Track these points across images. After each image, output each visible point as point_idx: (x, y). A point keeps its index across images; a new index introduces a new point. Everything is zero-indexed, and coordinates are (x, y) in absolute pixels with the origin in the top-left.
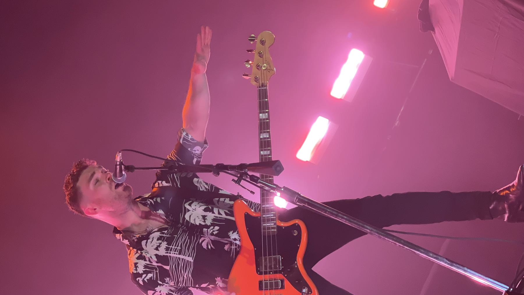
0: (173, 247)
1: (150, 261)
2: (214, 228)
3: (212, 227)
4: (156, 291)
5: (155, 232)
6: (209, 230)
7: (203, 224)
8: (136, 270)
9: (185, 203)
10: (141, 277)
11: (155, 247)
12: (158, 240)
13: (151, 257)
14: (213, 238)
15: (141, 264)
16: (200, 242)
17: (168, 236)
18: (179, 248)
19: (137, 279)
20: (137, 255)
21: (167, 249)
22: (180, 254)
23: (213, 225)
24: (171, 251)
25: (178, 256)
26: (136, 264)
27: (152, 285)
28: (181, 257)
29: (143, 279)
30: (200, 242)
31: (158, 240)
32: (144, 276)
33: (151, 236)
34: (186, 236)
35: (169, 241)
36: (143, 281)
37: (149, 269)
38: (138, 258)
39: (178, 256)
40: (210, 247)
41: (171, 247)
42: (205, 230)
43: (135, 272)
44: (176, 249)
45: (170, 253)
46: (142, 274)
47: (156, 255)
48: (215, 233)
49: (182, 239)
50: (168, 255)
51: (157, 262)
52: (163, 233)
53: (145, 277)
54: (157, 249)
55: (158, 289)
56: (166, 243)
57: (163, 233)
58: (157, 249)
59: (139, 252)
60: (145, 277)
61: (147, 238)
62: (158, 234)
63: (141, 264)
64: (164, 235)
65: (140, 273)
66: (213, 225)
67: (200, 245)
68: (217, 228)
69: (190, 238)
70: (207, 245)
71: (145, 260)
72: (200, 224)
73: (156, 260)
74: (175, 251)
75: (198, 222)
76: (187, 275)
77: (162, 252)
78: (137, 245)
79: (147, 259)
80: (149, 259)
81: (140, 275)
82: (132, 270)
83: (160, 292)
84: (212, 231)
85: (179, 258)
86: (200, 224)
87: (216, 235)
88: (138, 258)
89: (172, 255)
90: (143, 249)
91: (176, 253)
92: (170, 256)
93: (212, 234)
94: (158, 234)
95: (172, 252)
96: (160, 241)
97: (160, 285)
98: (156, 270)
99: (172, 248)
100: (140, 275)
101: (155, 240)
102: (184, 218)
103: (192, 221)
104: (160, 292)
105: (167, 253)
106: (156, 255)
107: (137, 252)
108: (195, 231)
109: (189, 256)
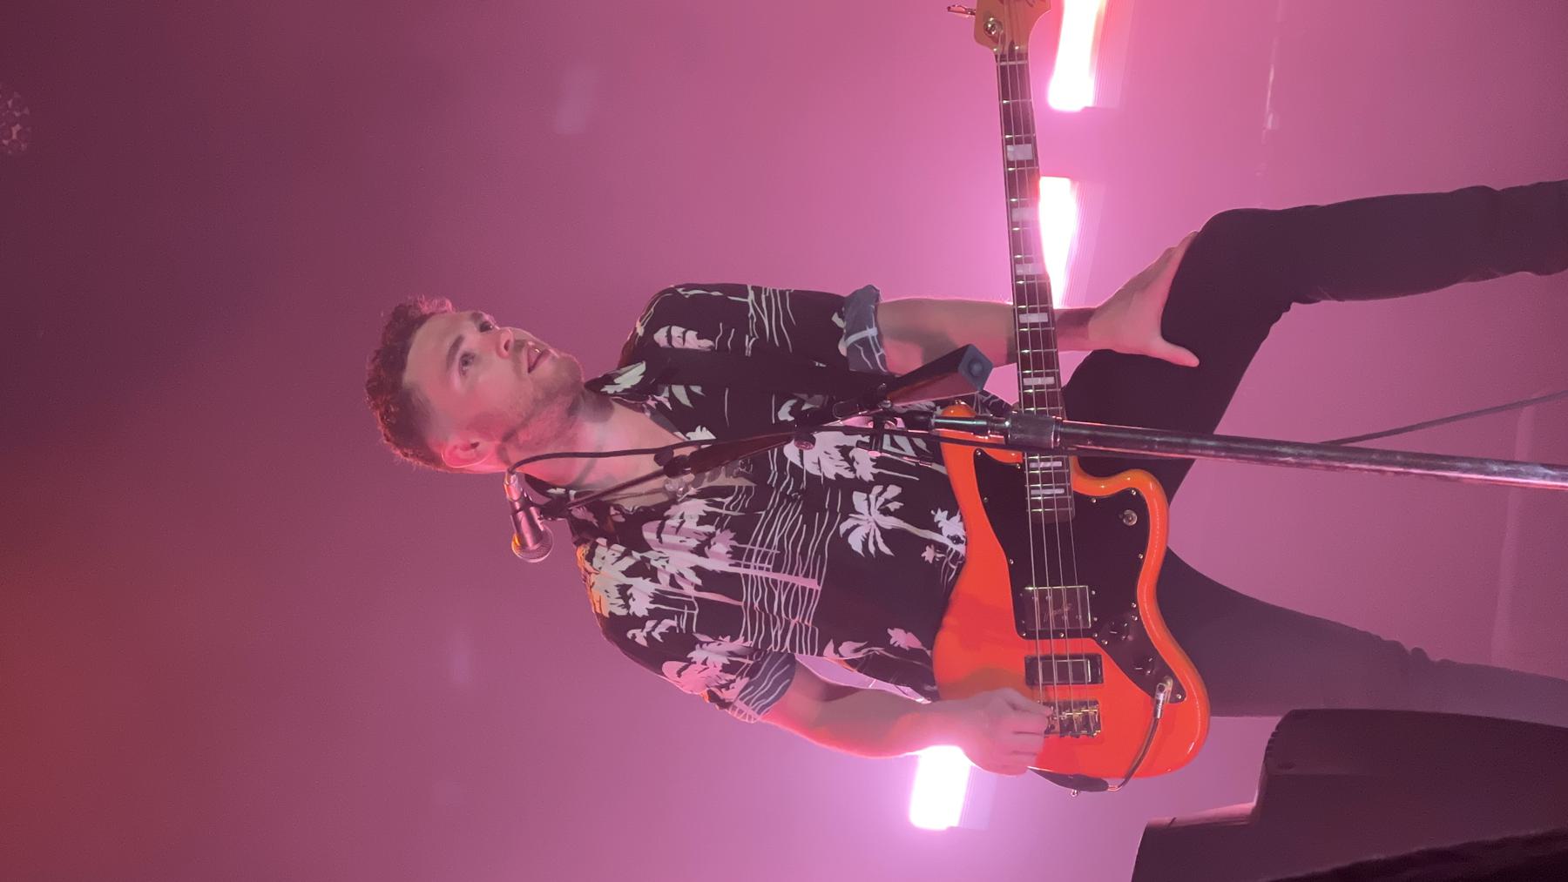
0: (756, 548)
1: (673, 582)
2: (884, 490)
3: (877, 489)
4: (690, 662)
6: (872, 497)
7: (848, 475)
8: (627, 606)
9: (778, 409)
11: (693, 543)
12: (699, 524)
13: (682, 575)
14: (891, 523)
15: (643, 591)
17: (736, 513)
19: (629, 635)
20: (627, 562)
21: (736, 554)
22: (777, 569)
23: (880, 480)
24: (749, 558)
25: (772, 575)
26: (624, 591)
27: (679, 647)
28: (781, 577)
29: (649, 633)
30: (844, 528)
31: (699, 524)
32: (650, 624)
33: (674, 511)
34: (795, 515)
35: (742, 529)
36: (649, 637)
38: (629, 573)
39: (772, 575)
40: (872, 549)
41: (749, 546)
42: (858, 498)
43: (622, 612)
44: (765, 554)
45: (747, 567)
46: (644, 619)
47: (698, 570)
48: (894, 506)
50: (741, 571)
51: (697, 588)
52: (720, 505)
54: (699, 551)
55: (697, 655)
57: (720, 505)
58: (699, 551)
59: (637, 556)
61: (657, 513)
62: (698, 507)
63: (643, 591)
64: (724, 511)
65: (639, 614)
66: (880, 480)
67: (841, 542)
68: (894, 490)
69: (808, 521)
70: (865, 544)
71: (655, 580)
72: (837, 475)
73: (699, 582)
74: (763, 561)
75: (832, 468)
77: (718, 561)
78: (629, 534)
79: (664, 579)
80: (672, 576)
81: (639, 622)
83: (704, 663)
84: (882, 500)
85: (775, 582)
86: (837, 475)
87: (896, 514)
88: (629, 573)
90: (646, 547)
91: (766, 565)
92: (746, 576)
93: (885, 511)
94: (698, 507)
95: (752, 564)
96: (709, 529)
97: (701, 643)
99: (751, 551)
100: (639, 622)
101: (691, 524)
102: (782, 459)
103: (810, 467)
104: (704, 663)
105: (738, 565)
106: (698, 570)
109: (806, 576)
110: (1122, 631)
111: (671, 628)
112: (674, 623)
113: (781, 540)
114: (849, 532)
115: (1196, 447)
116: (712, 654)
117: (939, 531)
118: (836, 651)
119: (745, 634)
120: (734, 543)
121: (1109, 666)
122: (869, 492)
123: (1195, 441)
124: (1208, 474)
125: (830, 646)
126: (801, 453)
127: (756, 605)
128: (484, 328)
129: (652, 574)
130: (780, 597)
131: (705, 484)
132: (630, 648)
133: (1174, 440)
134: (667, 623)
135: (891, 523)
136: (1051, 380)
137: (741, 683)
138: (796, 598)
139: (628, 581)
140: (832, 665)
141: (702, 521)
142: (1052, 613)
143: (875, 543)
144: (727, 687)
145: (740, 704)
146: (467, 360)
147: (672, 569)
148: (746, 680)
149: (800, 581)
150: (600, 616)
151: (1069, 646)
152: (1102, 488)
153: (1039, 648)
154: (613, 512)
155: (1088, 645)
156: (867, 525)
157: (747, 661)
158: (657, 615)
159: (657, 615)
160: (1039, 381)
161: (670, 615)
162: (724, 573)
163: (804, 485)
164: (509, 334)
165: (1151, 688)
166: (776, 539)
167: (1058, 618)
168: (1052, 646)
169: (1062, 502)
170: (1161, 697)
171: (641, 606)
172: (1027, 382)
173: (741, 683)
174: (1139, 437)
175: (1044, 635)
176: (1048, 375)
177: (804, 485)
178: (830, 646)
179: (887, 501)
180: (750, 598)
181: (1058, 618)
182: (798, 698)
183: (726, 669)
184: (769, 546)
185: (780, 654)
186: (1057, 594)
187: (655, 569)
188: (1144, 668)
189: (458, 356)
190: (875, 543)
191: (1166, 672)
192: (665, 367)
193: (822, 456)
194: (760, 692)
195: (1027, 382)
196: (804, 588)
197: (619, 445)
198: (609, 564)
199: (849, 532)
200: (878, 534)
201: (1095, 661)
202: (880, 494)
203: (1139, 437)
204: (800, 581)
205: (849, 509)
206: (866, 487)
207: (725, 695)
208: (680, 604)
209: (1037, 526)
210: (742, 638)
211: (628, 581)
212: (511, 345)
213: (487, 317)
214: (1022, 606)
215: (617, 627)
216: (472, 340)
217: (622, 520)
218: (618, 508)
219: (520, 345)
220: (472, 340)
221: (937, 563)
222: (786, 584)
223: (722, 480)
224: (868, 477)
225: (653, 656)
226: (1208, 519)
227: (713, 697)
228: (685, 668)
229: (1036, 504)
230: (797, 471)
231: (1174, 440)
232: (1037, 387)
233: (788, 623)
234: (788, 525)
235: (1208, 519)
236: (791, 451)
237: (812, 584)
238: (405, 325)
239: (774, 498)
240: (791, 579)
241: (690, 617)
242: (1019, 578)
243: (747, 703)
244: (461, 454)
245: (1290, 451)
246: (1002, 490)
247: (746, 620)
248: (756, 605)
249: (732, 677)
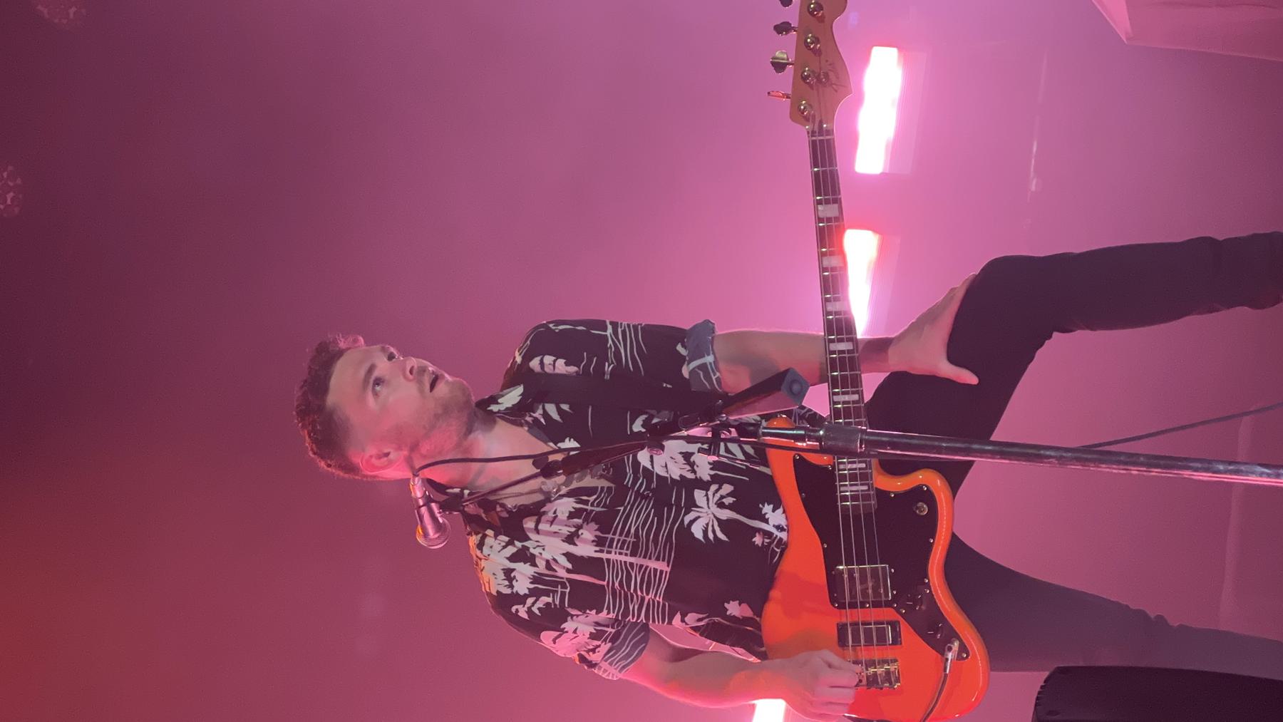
0: (617, 537)
1: (548, 566)
3: (714, 487)
4: (563, 631)
5: (562, 496)
6: (710, 493)
7: (690, 476)
8: (511, 586)
9: (633, 422)
10: (524, 603)
13: (555, 560)
14: (726, 514)
16: (686, 522)
18: (631, 539)
20: (511, 550)
21: (599, 542)
22: (633, 554)
24: (610, 546)
25: (630, 559)
26: (508, 573)
27: (554, 619)
29: (529, 608)
30: (687, 519)
32: (530, 601)
33: (550, 508)
35: (604, 522)
36: (529, 611)
37: (543, 583)
39: (630, 559)
40: (711, 536)
41: (610, 536)
43: (508, 591)
44: (624, 542)
45: (609, 552)
46: (526, 596)
47: (568, 555)
49: (637, 518)
50: (604, 556)
51: (568, 571)
52: (586, 502)
53: (533, 604)
54: (570, 539)
55: (569, 625)
56: (594, 526)
57: (586, 502)
58: (570, 539)
59: (519, 544)
60: (533, 604)
61: (536, 510)
62: (565, 506)
63: (524, 571)
64: (589, 508)
65: (522, 593)
66: (715, 479)
67: (686, 531)
68: (727, 488)
69: (659, 515)
70: (705, 532)
71: (534, 565)
72: (681, 476)
73: (570, 566)
74: (622, 548)
75: (677, 471)
76: (656, 596)
77: (585, 549)
78: (512, 525)
79: (541, 564)
80: (548, 561)
81: (521, 599)
82: (497, 585)
83: (575, 632)
84: (718, 495)
85: (632, 564)
86: (681, 476)
87: (730, 507)
88: (513, 558)
89: (612, 557)
90: (528, 539)
92: (608, 560)
93: (721, 505)
96: (579, 521)
97: (572, 616)
98: (564, 586)
99: (612, 540)
100: (521, 599)
102: (636, 464)
103: (659, 470)
104: (575, 632)
105: (602, 551)
106: (568, 555)
107: (508, 544)
108: (673, 496)
109: (658, 559)
110: (916, 602)
111: (548, 604)
112: (550, 600)
113: (637, 530)
114: (692, 522)
116: (580, 626)
117: (766, 521)
118: (683, 621)
119: (608, 608)
120: (598, 533)
121: (906, 630)
122: (707, 490)
123: (976, 446)
124: (984, 469)
125: (678, 616)
126: (652, 457)
127: (617, 584)
129: (531, 560)
130: (636, 577)
131: (575, 485)
132: (515, 620)
133: (958, 445)
134: (545, 599)
135: (726, 514)
136: (856, 397)
137: (605, 647)
138: (649, 580)
139: (512, 565)
140: (681, 630)
141: (572, 515)
142: (858, 587)
143: (714, 531)
144: (593, 651)
145: (605, 665)
147: (547, 555)
148: (609, 645)
149: (653, 564)
150: (489, 594)
151: (873, 614)
152: (898, 485)
153: (848, 616)
154: (499, 509)
155: (888, 614)
156: (707, 517)
157: (610, 630)
158: (535, 593)
159: (535, 593)
160: (846, 398)
161: (547, 593)
162: (590, 558)
163: (654, 485)
164: (413, 362)
165: (941, 648)
166: (633, 530)
167: (864, 592)
168: (859, 615)
169: (866, 497)
170: (950, 656)
171: (522, 586)
172: (836, 398)
173: (605, 647)
174: (928, 443)
175: (853, 606)
176: (853, 393)
177: (654, 485)
178: (678, 616)
179: (722, 497)
180: (611, 580)
181: (864, 592)
182: (651, 659)
183: (593, 636)
184: (627, 536)
185: (636, 624)
186: (863, 572)
187: (533, 556)
188: (936, 632)
190: (714, 531)
191: (952, 635)
192: (540, 390)
193: (667, 460)
194: (621, 654)
195: (836, 398)
196: (655, 570)
197: (505, 454)
198: (495, 554)
199: (692, 522)
200: (716, 524)
201: (894, 625)
202: (717, 491)
203: (928, 443)
204: (653, 564)
205: (691, 504)
206: (704, 486)
207: (593, 657)
208: (555, 584)
209: (846, 517)
210: (605, 611)
211: (512, 565)
214: (834, 581)
215: (504, 602)
216: (383, 367)
217: (505, 515)
218: (503, 506)
219: (423, 370)
220: (383, 367)
221: (765, 548)
222: (641, 566)
223: (588, 481)
224: (706, 478)
225: (534, 626)
226: (987, 509)
227: (583, 659)
228: (559, 636)
229: (845, 498)
230: (648, 473)
231: (958, 445)
232: (844, 403)
233: (643, 599)
234: (642, 517)
235: (987, 509)
236: (643, 457)
237: (662, 566)
238: (326, 359)
239: (630, 497)
240: (646, 562)
241: (563, 594)
242: (831, 560)
243: (611, 664)
244: (374, 461)
245: (1052, 453)
246: (816, 487)
247: (609, 597)
248: (617, 584)
249: (597, 643)
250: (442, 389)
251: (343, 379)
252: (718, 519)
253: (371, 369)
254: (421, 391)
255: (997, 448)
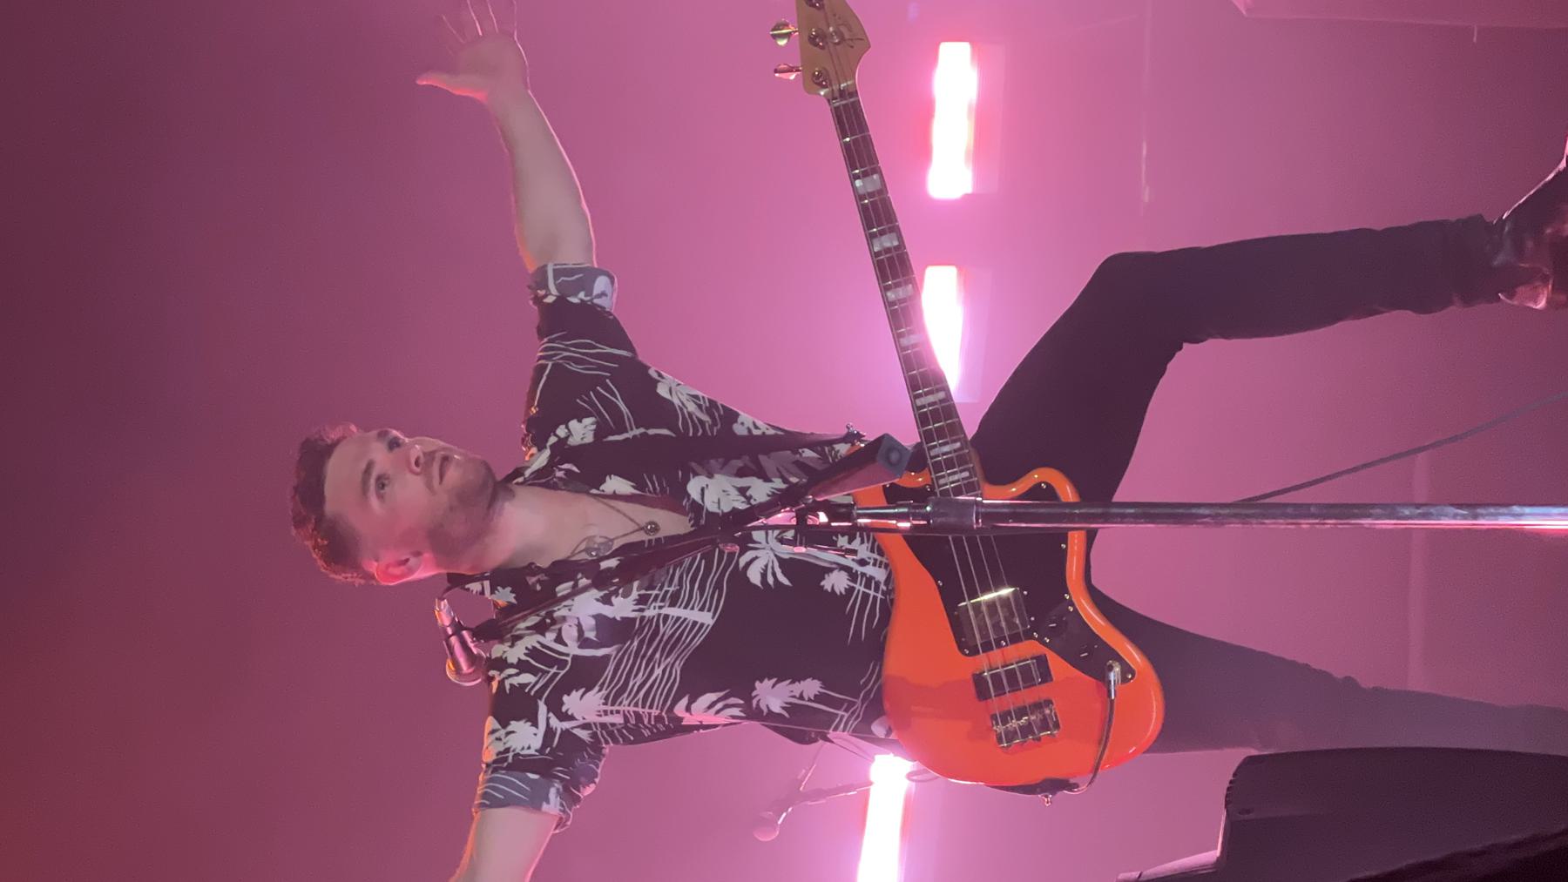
30: (743, 561)
40: (770, 580)
67: (740, 576)
70: (764, 576)
103: (710, 505)
113: (681, 578)
115: (1118, 515)
128: (394, 444)
136: (958, 445)
146: (382, 482)
160: (946, 449)
163: (703, 522)
164: (416, 448)
172: (919, 402)
177: (703, 522)
189: (372, 481)
195: (919, 402)
212: (422, 460)
213: (395, 433)
219: (430, 456)
232: (930, 405)
250: (453, 475)
251: (339, 472)
252: (780, 560)
253: (370, 466)
254: (429, 486)
255: (1140, 511)
